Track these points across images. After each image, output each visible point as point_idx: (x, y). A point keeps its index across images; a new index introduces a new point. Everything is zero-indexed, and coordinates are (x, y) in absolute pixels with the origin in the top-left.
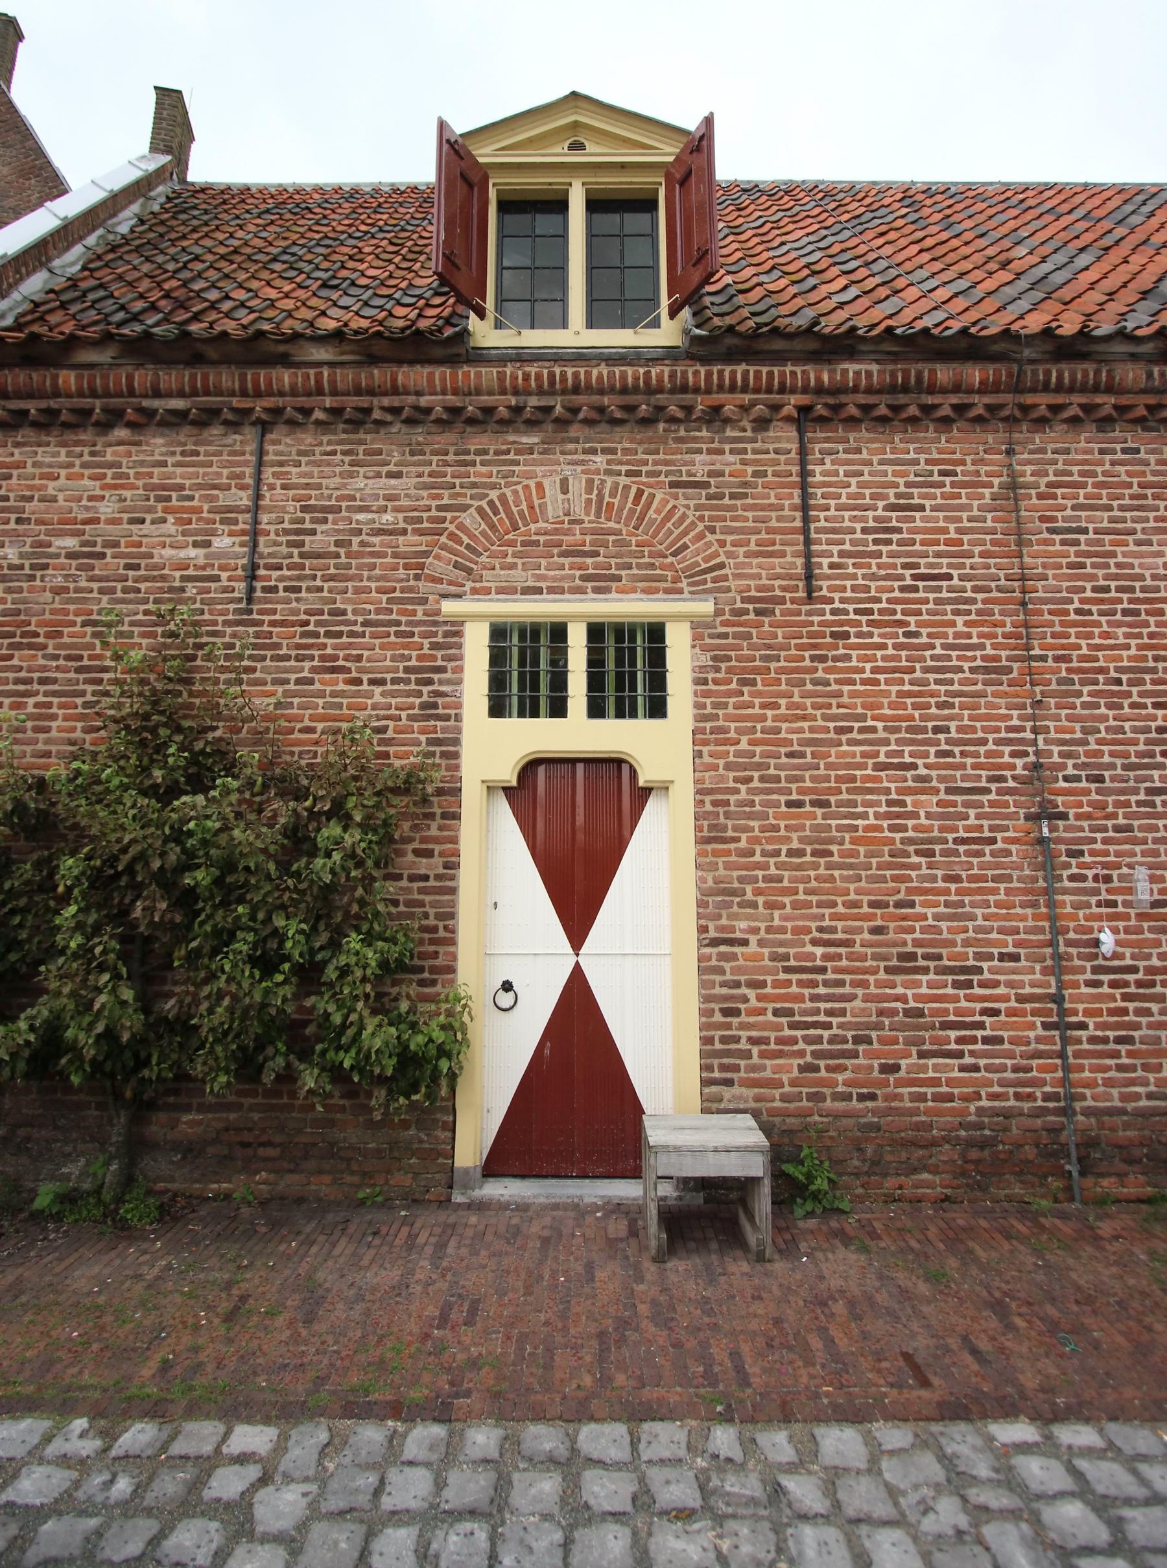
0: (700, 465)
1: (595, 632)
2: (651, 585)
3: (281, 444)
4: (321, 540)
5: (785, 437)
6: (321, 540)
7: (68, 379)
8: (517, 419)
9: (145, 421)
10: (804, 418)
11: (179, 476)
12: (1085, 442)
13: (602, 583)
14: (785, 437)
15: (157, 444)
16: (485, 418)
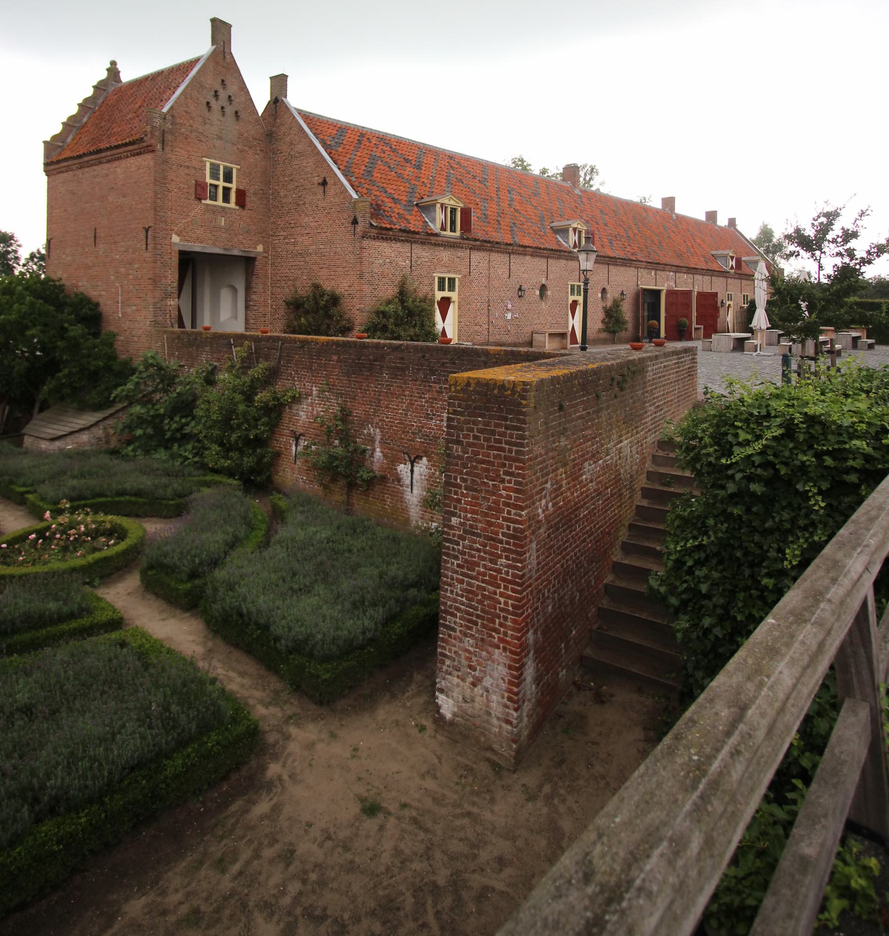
0: (459, 254)
1: (449, 279)
2: (455, 273)
3: (414, 246)
4: (419, 263)
5: (468, 251)
6: (419, 263)
7: (391, 233)
8: (442, 245)
9: (399, 241)
10: (471, 249)
11: (401, 250)
12: (496, 255)
13: (449, 272)
14: (468, 251)
15: (399, 245)
16: (439, 245)
